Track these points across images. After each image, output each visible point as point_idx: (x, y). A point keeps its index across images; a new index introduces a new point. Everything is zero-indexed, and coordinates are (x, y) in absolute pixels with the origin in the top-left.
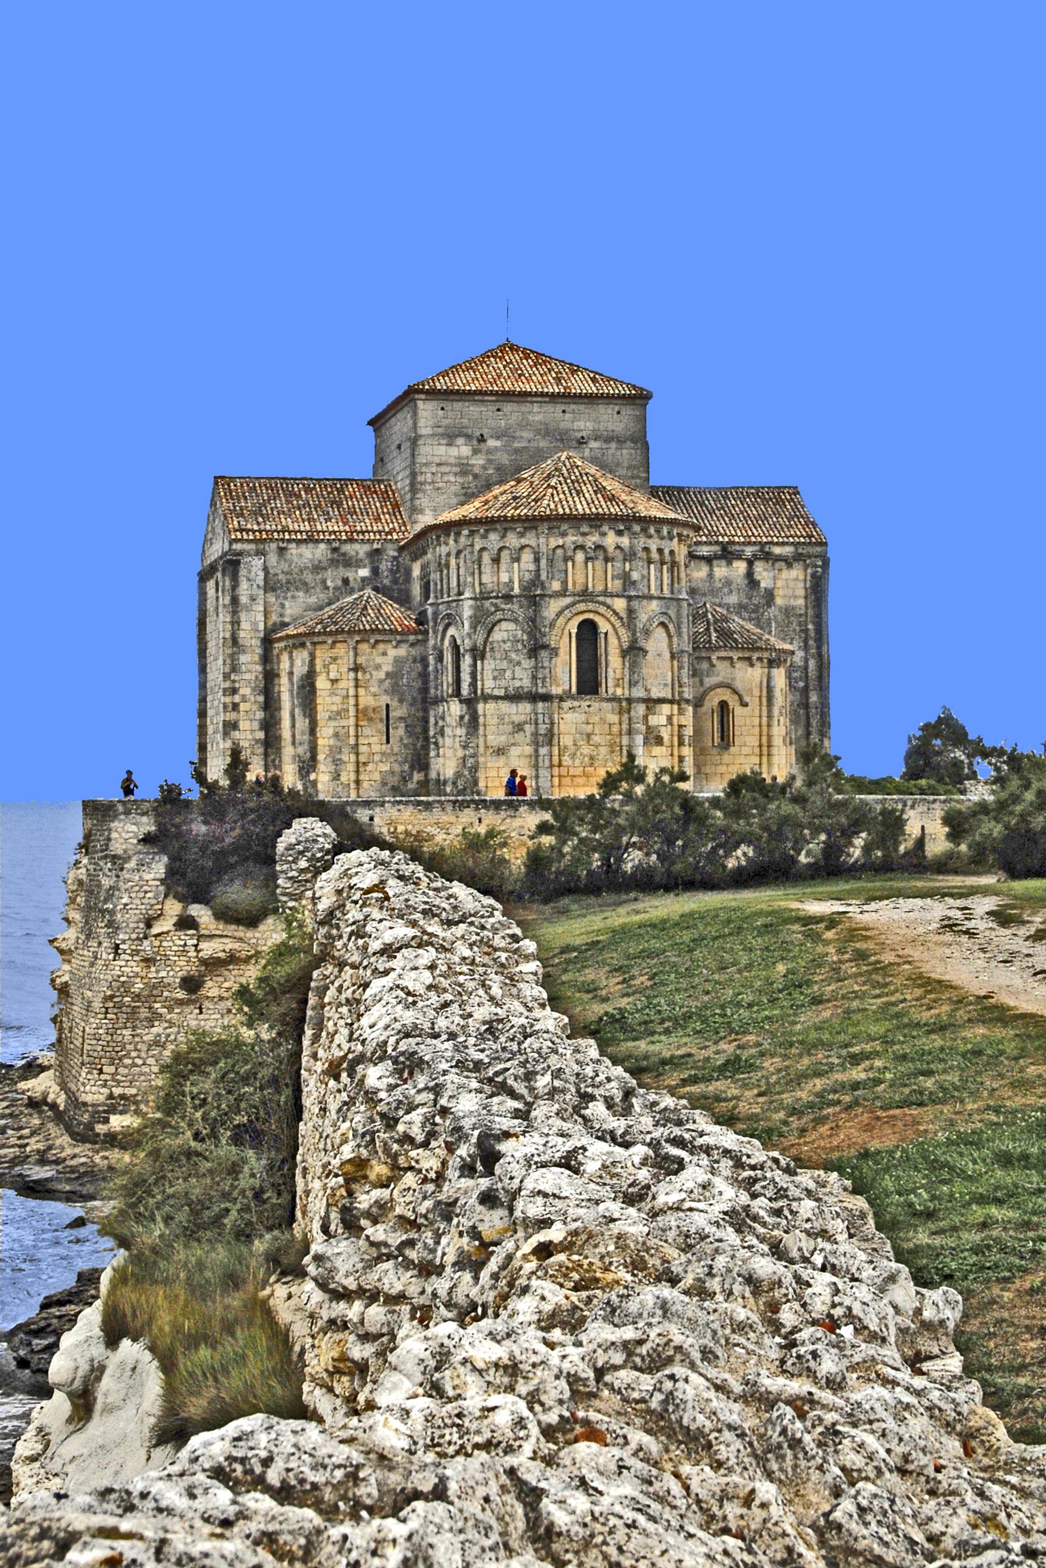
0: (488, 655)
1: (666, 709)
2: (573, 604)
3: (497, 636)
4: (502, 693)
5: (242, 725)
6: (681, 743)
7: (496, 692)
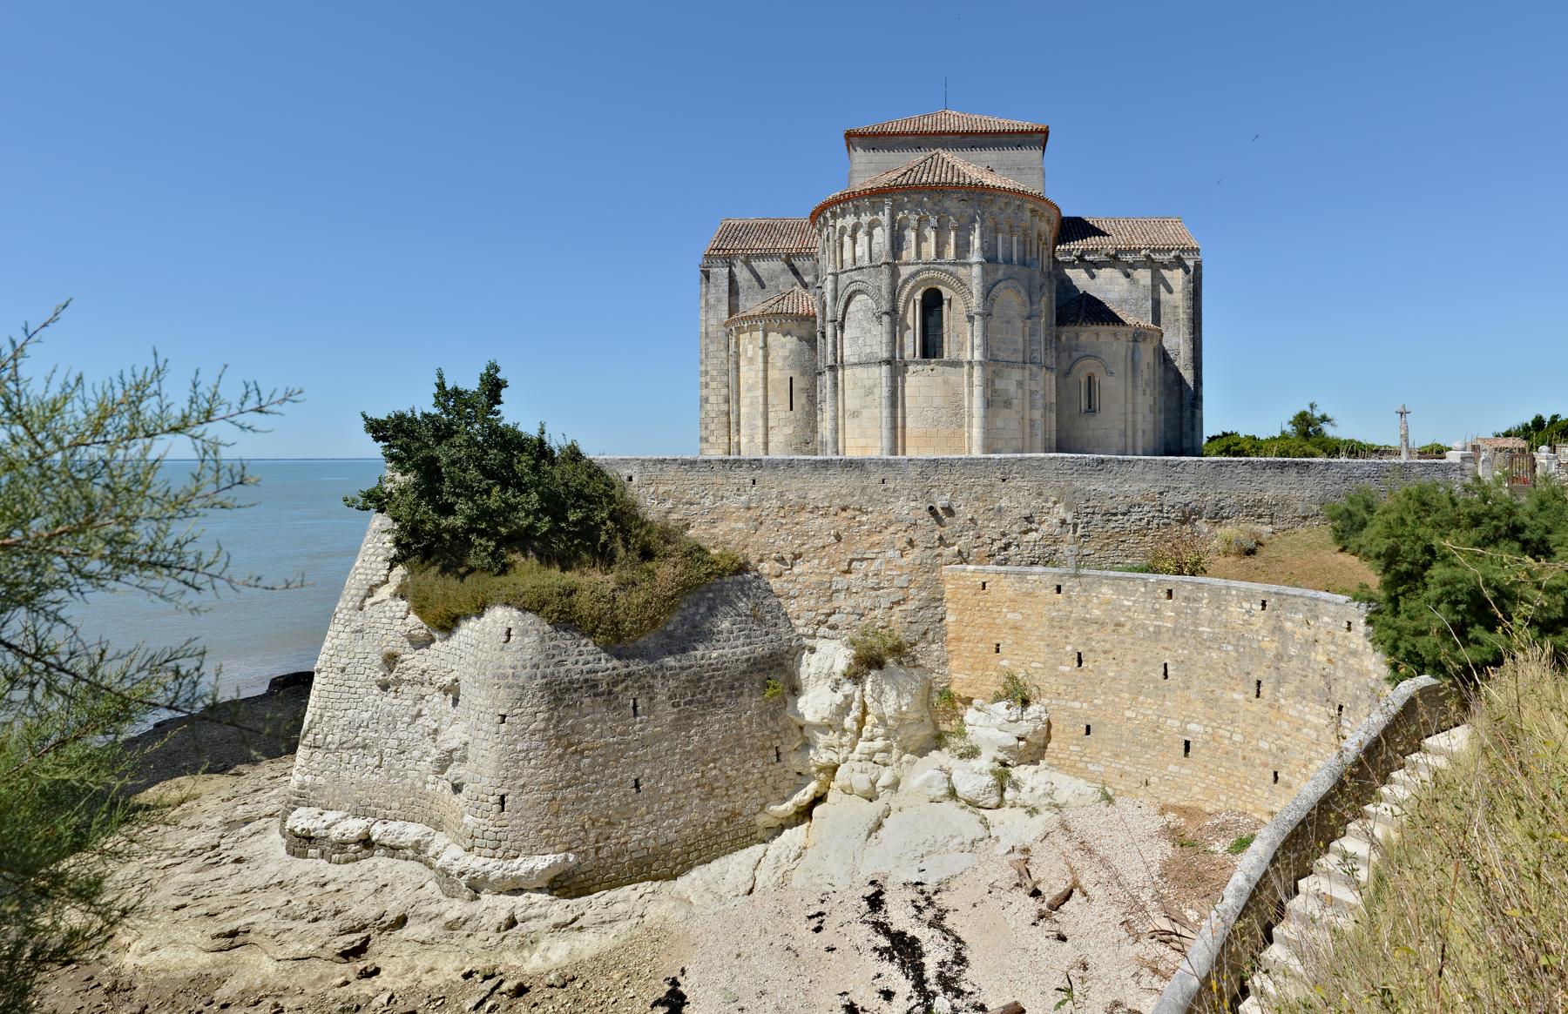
1: (1016, 374)
2: (917, 273)
3: (852, 307)
5: (712, 399)
6: (1032, 407)
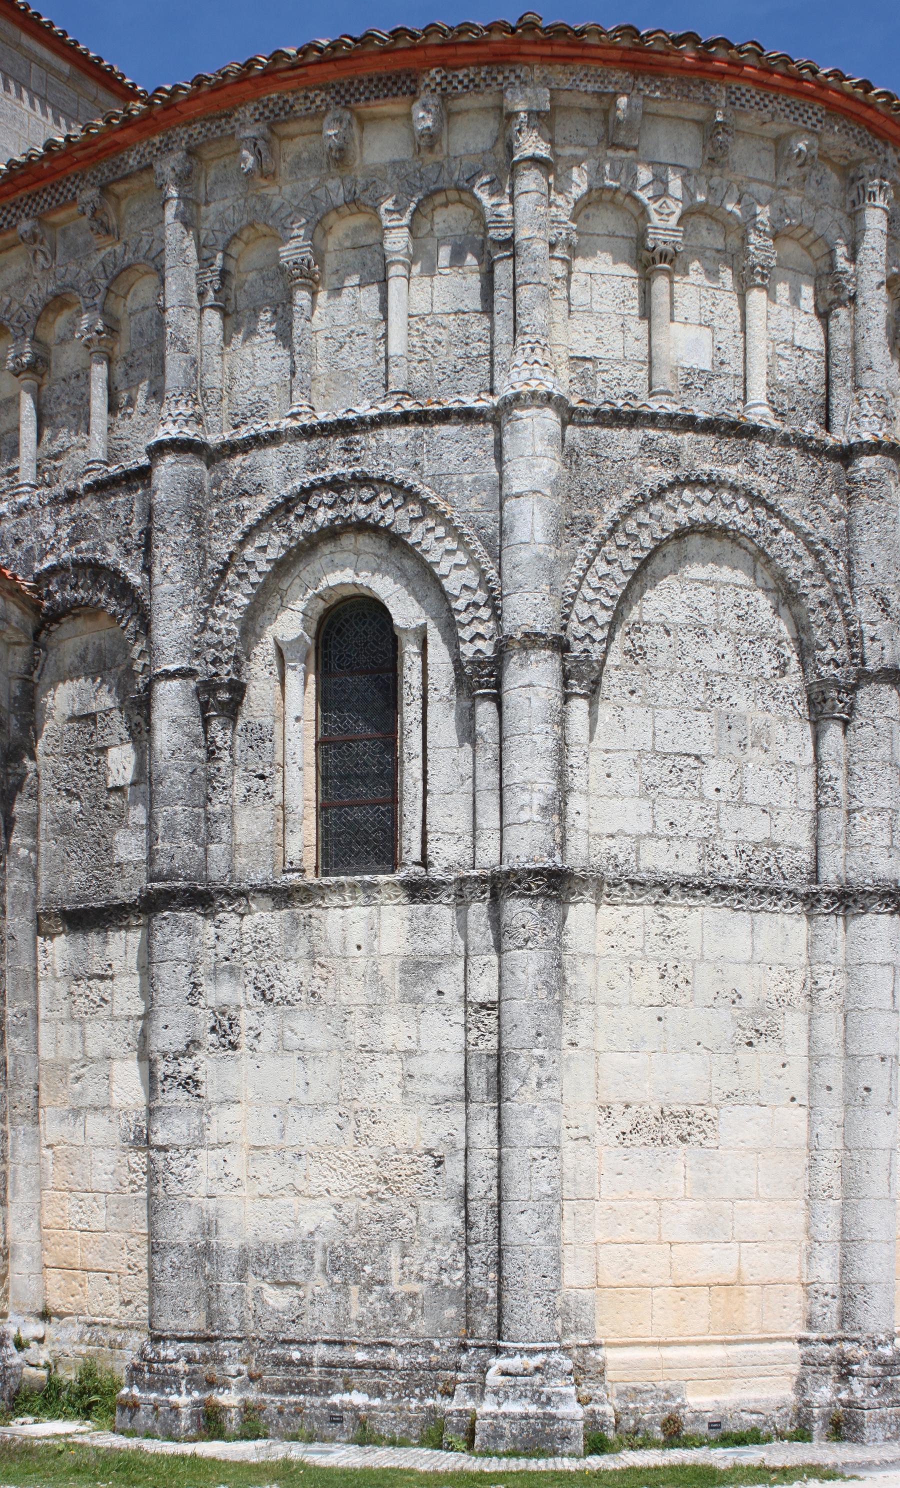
0: (612, 681)
4: (688, 865)
7: (658, 859)
